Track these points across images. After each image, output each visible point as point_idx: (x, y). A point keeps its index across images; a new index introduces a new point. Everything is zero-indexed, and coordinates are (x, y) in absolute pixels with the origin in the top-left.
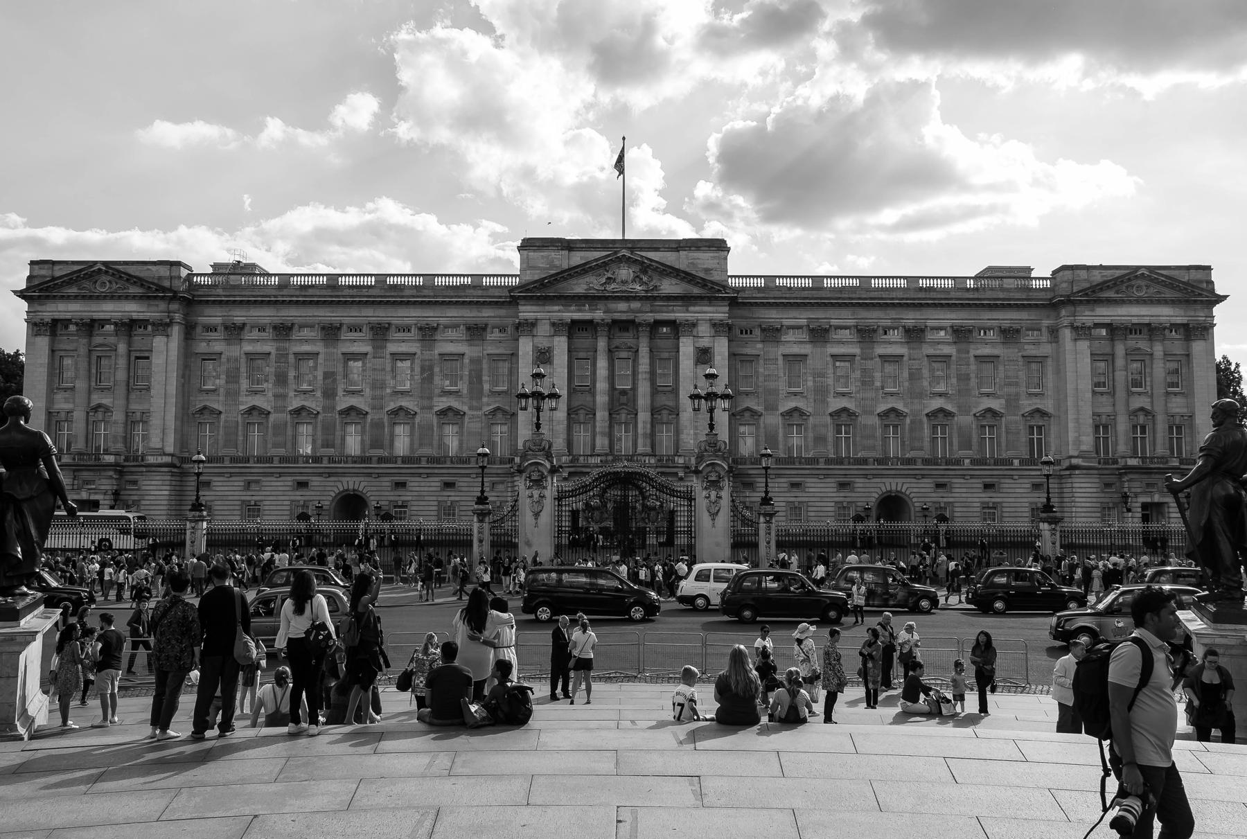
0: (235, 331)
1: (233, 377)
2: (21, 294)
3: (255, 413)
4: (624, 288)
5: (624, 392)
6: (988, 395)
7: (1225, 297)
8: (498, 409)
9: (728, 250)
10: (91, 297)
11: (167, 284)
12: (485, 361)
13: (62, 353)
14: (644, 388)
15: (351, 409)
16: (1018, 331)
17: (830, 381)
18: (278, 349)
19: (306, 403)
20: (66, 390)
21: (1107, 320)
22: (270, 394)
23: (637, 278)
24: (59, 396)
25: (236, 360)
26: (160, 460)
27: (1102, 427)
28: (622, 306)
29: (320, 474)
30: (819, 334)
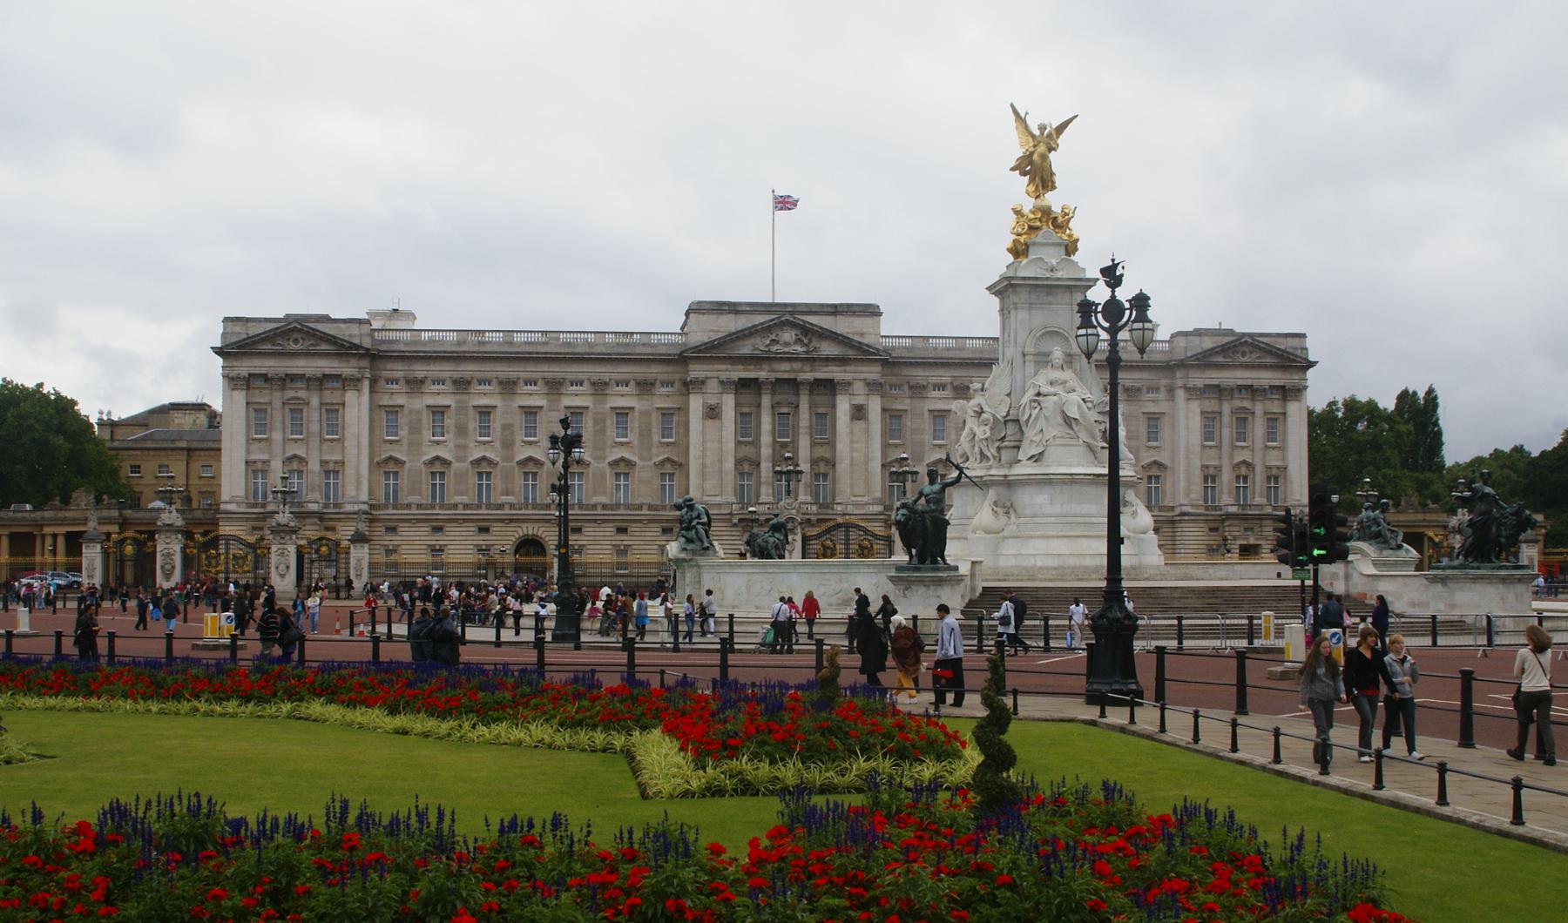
1: (415, 428)
2: (219, 351)
3: (438, 463)
5: (784, 445)
8: (668, 460)
9: (880, 314)
11: (356, 341)
14: (804, 442)
15: (530, 459)
16: (1139, 390)
19: (488, 455)
20: (260, 440)
21: (1215, 382)
22: (451, 445)
23: (798, 341)
24: (256, 446)
25: (418, 412)
26: (356, 508)
27: (1210, 478)
28: (785, 366)
29: (502, 521)
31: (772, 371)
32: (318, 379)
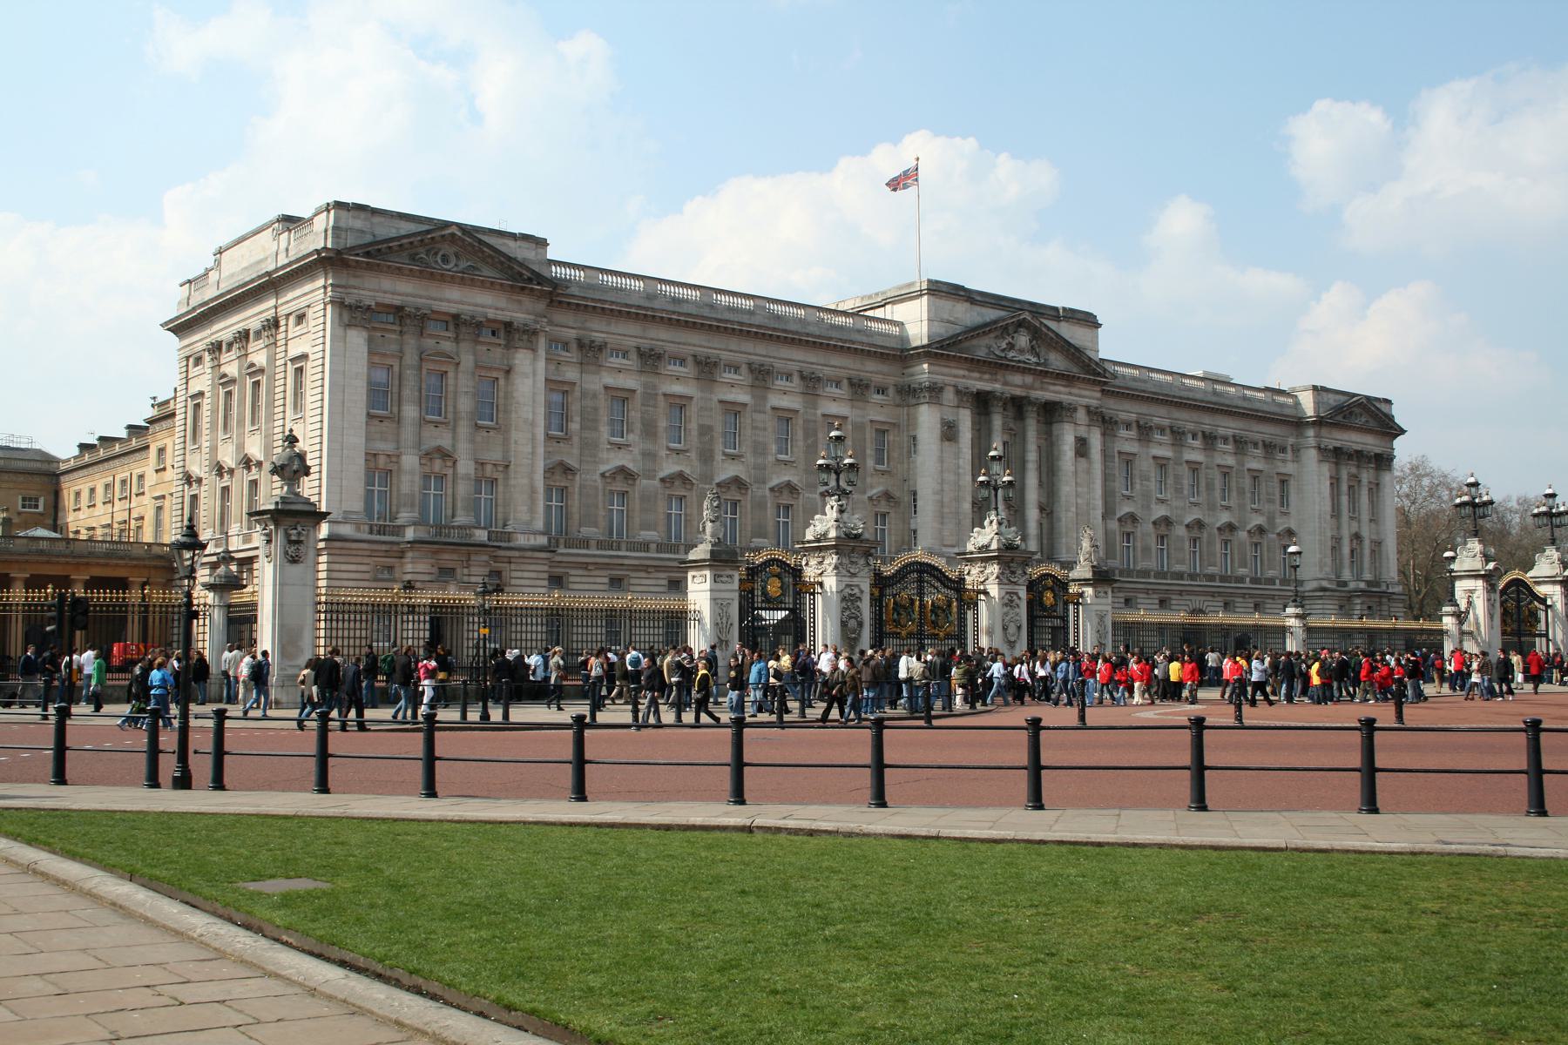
0: (591, 351)
1: (590, 423)
3: (619, 477)
4: (1021, 358)
6: (1256, 511)
7: (1403, 432)
10: (432, 276)
12: (868, 429)
13: (377, 359)
17: (1153, 485)
18: (645, 385)
21: (1338, 444)
22: (636, 451)
25: (595, 396)
28: (1017, 379)
30: (1145, 431)
31: (1005, 383)
32: (479, 325)
